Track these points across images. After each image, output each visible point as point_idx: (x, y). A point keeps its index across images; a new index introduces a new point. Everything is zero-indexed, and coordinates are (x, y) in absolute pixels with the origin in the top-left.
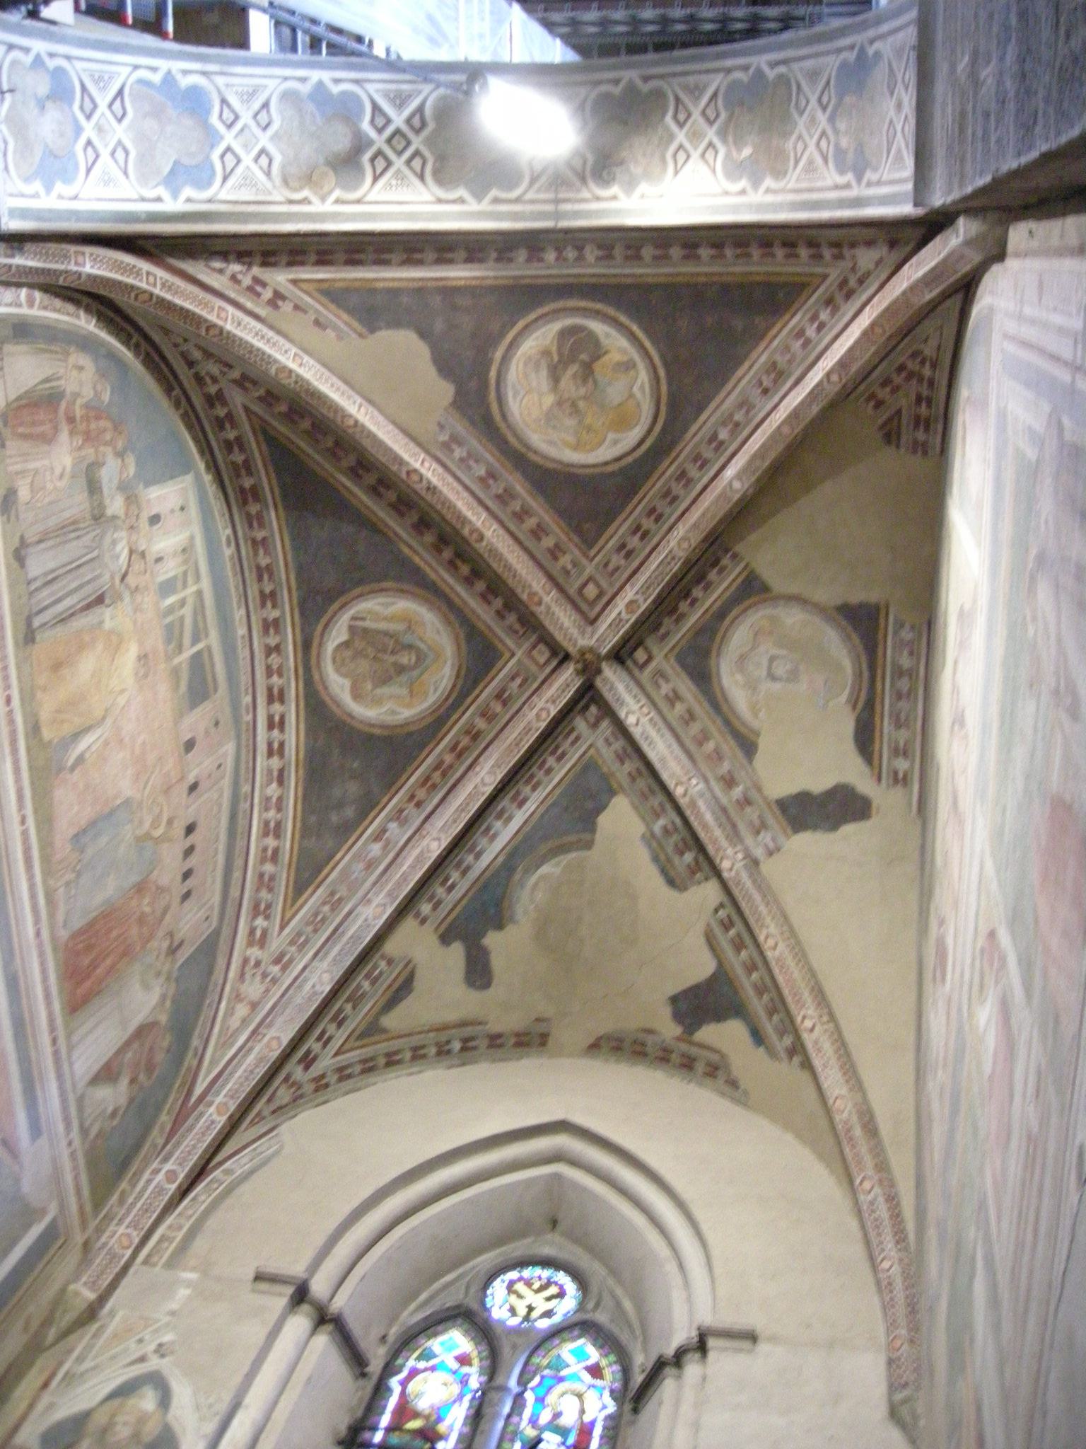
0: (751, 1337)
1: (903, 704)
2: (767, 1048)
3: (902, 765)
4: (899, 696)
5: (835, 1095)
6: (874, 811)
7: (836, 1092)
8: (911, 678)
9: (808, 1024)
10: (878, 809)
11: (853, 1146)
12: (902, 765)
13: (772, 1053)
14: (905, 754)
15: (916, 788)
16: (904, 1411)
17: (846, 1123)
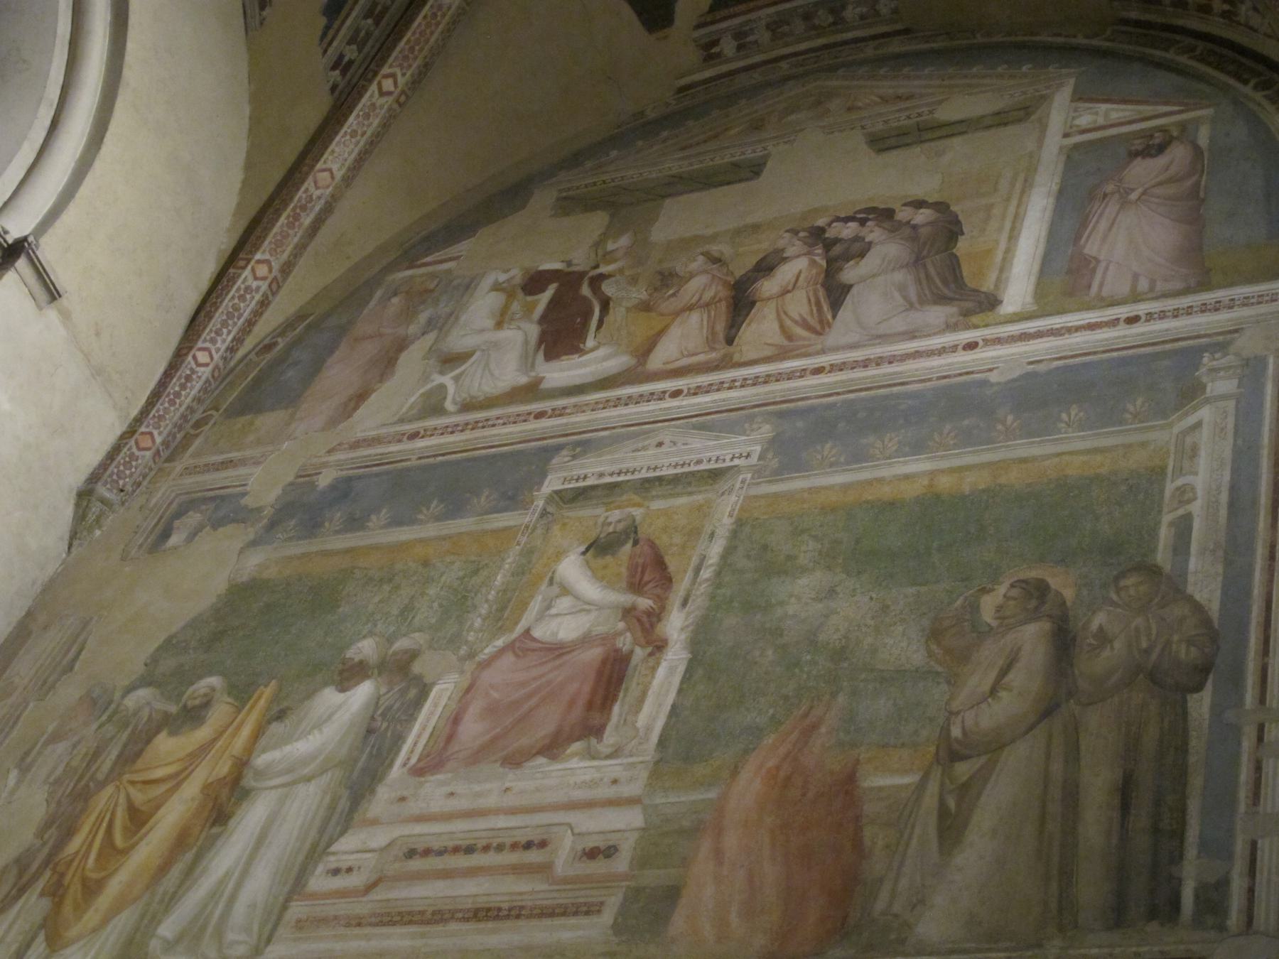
0: (53, 294)
1: (799, 26)
2: (327, 28)
3: (728, 47)
4: (807, 17)
5: (329, 165)
6: (661, 34)
7: (335, 167)
8: (834, 24)
9: (388, 85)
10: (666, 37)
11: (291, 225)
12: (728, 47)
13: (326, 36)
14: (740, 47)
15: (708, 74)
16: (96, 508)
17: (310, 199)
